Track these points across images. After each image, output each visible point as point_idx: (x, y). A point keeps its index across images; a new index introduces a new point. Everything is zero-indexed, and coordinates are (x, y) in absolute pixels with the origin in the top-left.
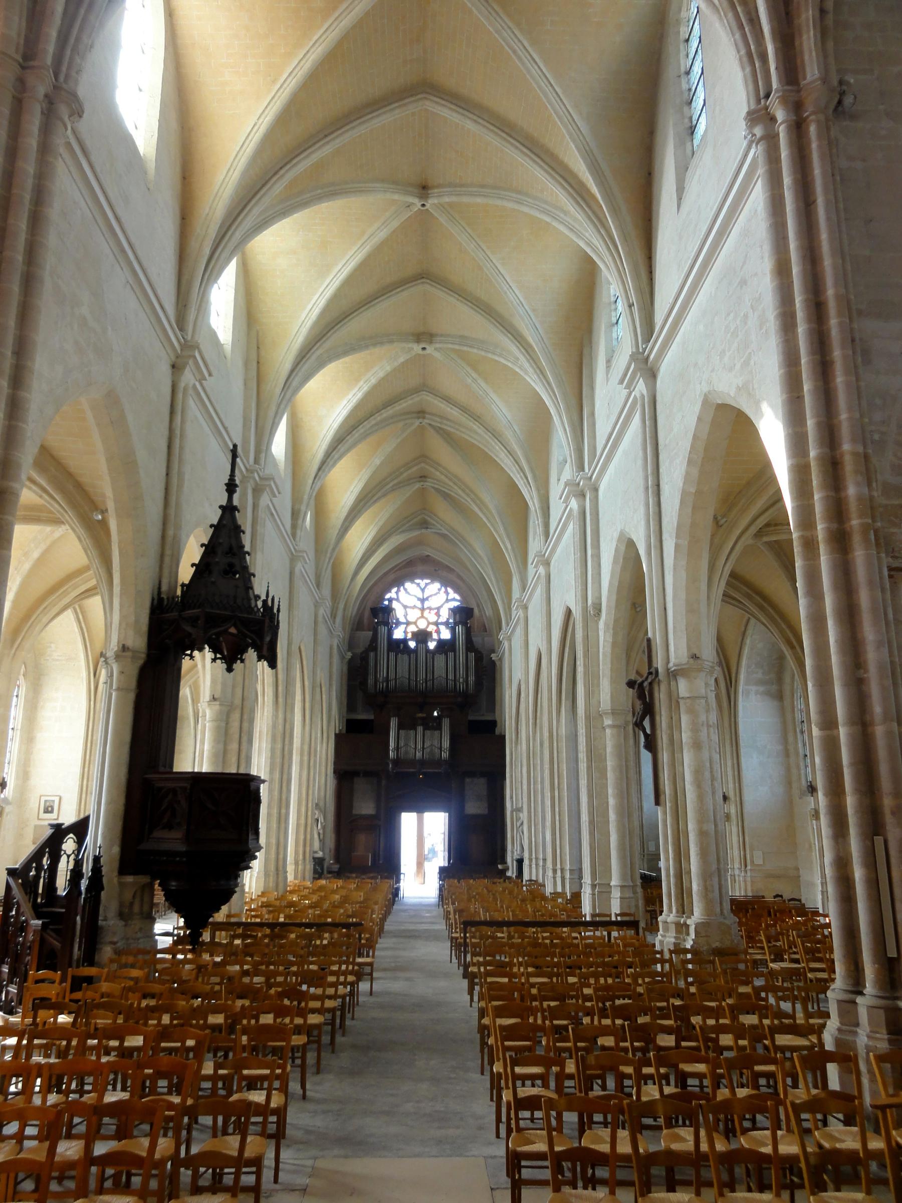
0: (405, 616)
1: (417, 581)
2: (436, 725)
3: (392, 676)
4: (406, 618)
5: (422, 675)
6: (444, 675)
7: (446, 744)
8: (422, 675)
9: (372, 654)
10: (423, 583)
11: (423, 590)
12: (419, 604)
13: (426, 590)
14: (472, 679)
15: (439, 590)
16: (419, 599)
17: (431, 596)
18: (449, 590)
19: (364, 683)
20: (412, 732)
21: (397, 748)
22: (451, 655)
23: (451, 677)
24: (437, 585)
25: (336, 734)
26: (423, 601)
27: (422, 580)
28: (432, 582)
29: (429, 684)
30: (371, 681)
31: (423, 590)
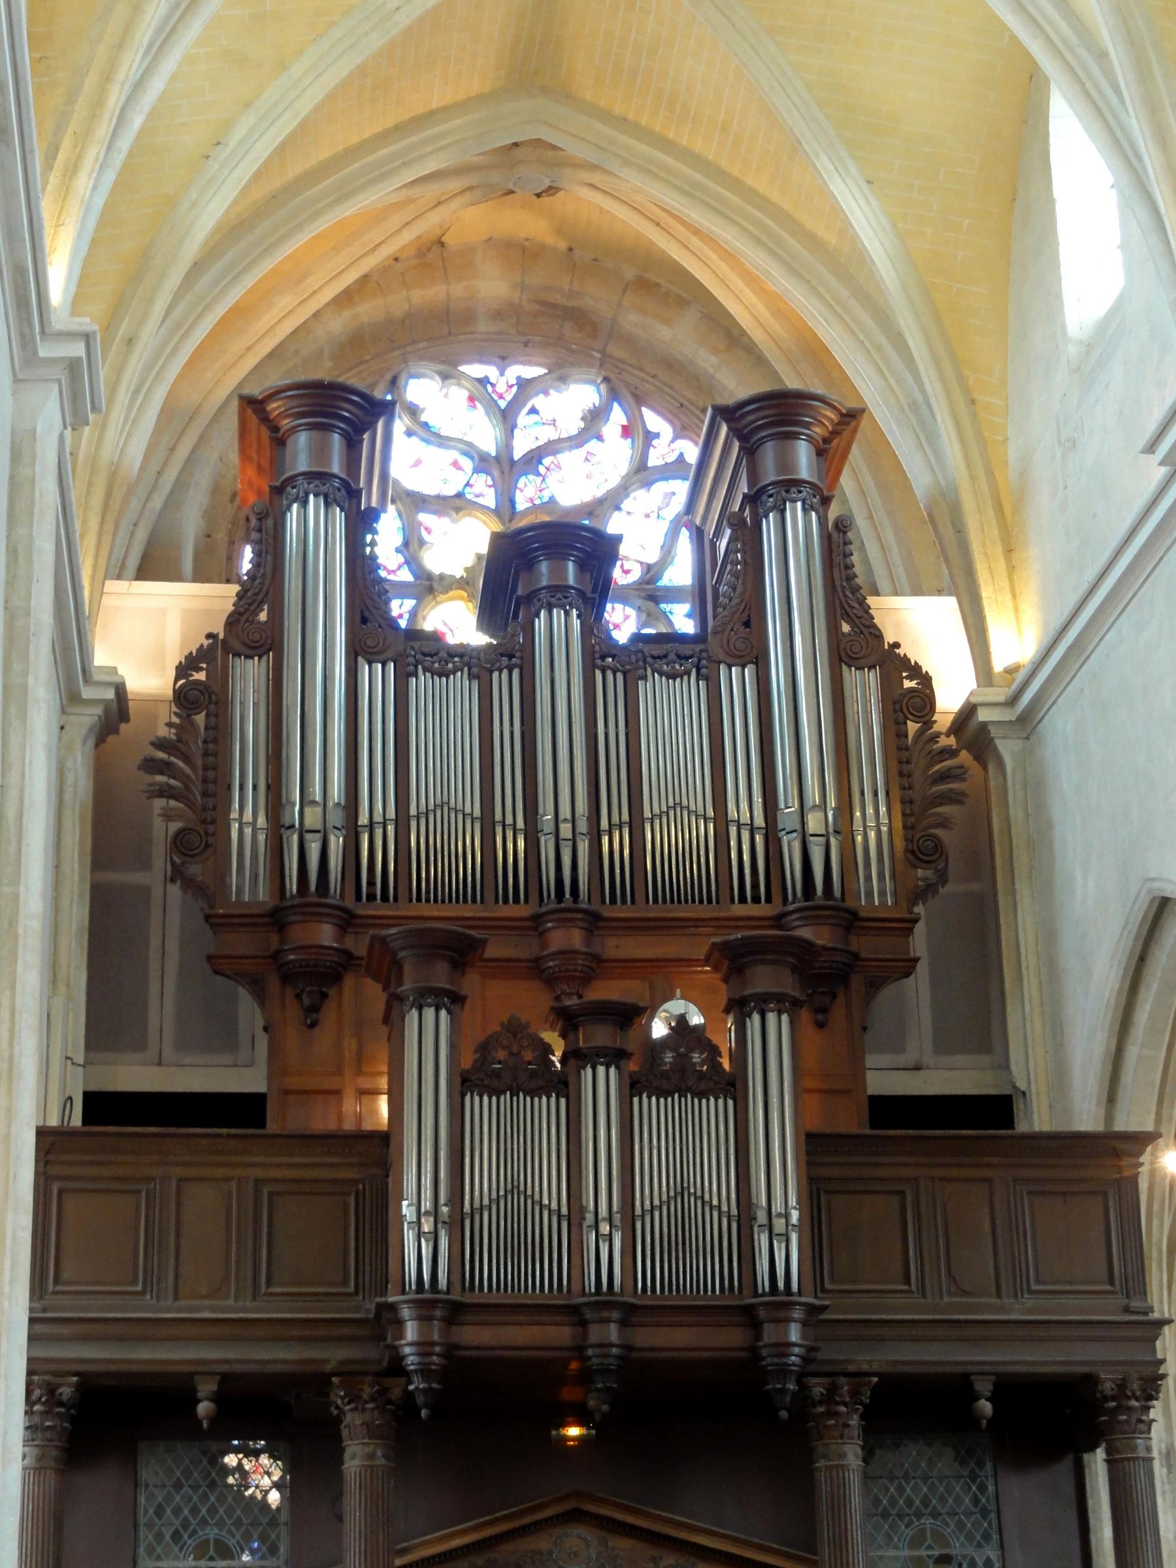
0: (411, 545)
1: (475, 370)
2: (694, 1073)
3: (377, 803)
4: (412, 562)
5: (564, 794)
6: (700, 798)
7: (781, 1189)
8: (564, 794)
9: (249, 677)
10: (503, 380)
11: (507, 418)
12: (484, 491)
13: (523, 419)
14: (875, 822)
15: (594, 419)
16: (483, 463)
17: (551, 448)
18: (653, 420)
19: (201, 841)
20: (547, 1109)
21: (457, 1219)
22: (737, 681)
23: (745, 806)
24: (577, 397)
25: (42, 1133)
26: (505, 467)
27: (503, 361)
28: (559, 375)
29: (616, 843)
30: (246, 818)
31: (507, 418)
